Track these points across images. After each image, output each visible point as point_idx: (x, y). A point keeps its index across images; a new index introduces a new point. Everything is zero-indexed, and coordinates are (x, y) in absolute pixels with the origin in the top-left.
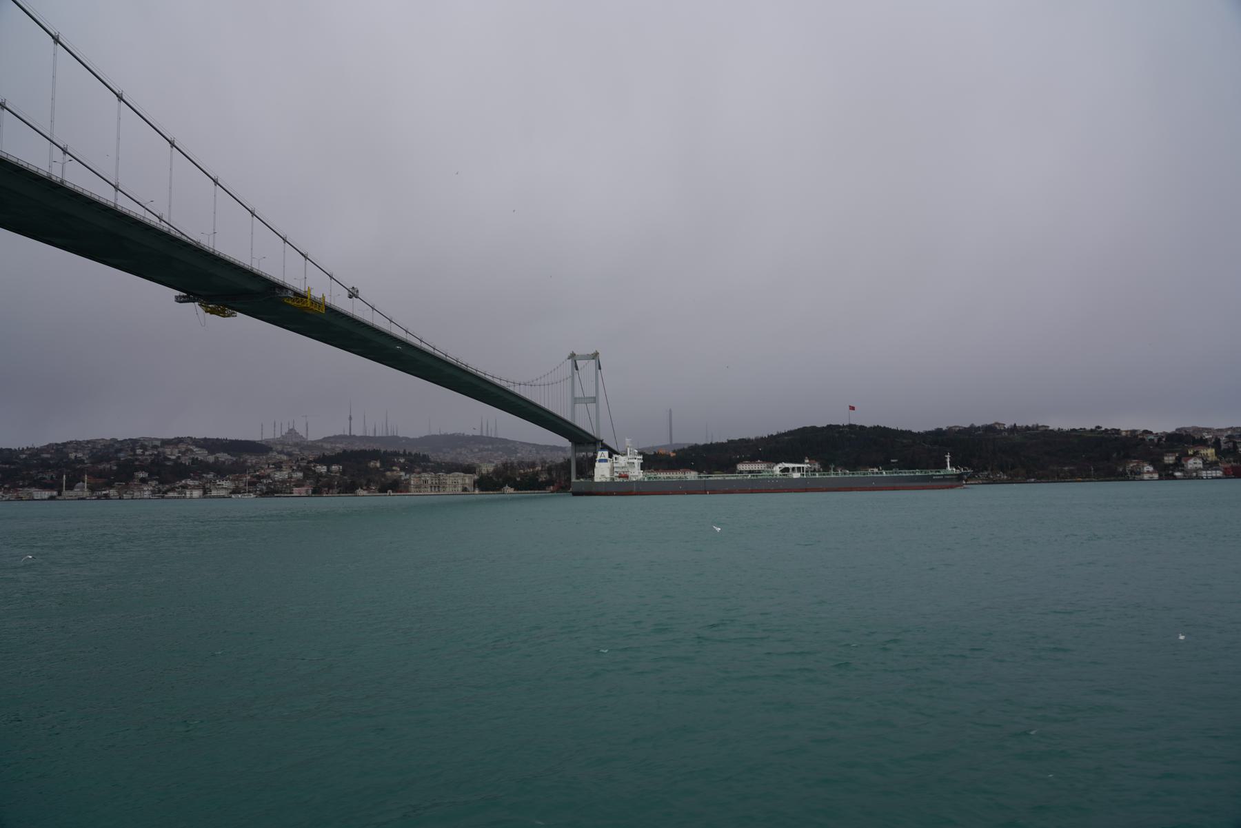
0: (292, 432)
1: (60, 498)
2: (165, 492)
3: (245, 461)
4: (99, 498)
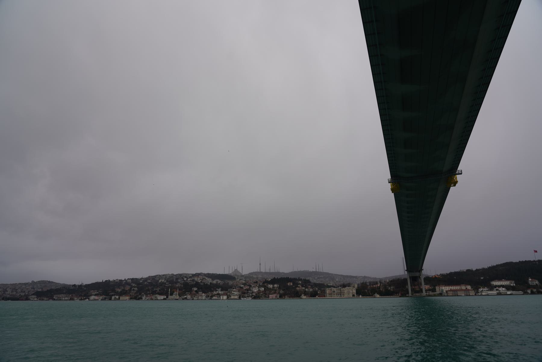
0: (236, 270)
1: (167, 299)
2: (212, 297)
3: (228, 284)
4: (183, 299)
